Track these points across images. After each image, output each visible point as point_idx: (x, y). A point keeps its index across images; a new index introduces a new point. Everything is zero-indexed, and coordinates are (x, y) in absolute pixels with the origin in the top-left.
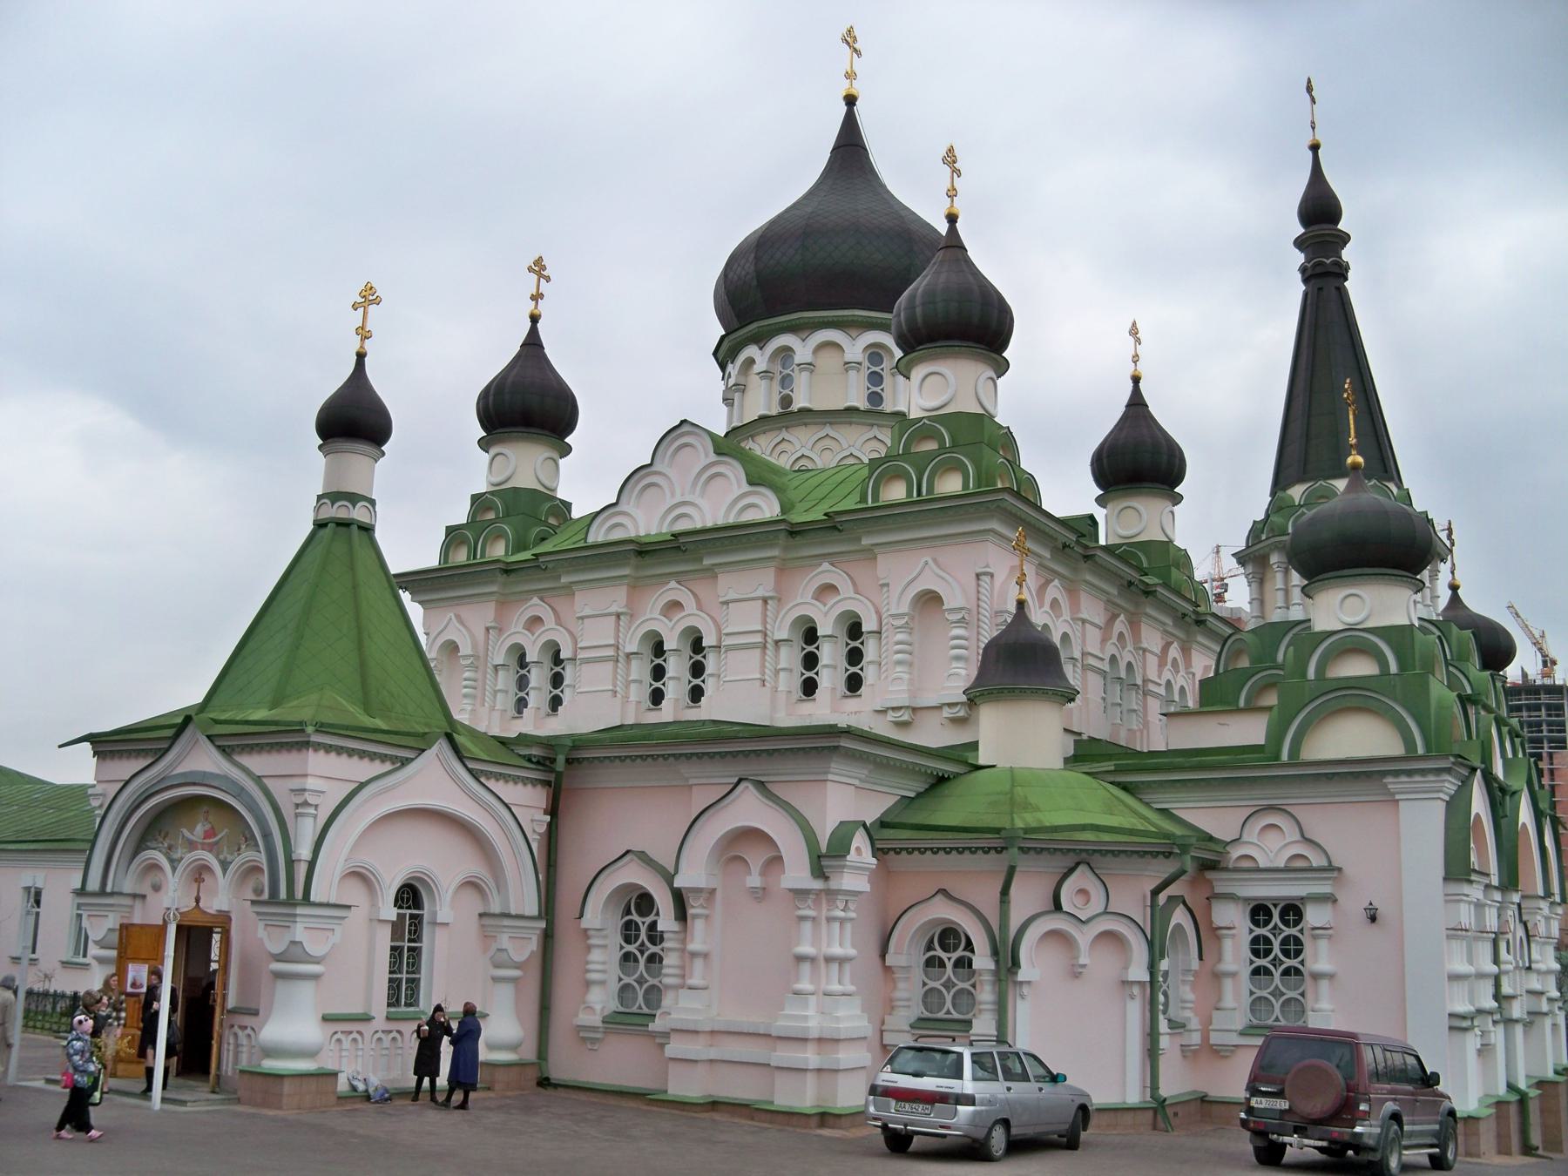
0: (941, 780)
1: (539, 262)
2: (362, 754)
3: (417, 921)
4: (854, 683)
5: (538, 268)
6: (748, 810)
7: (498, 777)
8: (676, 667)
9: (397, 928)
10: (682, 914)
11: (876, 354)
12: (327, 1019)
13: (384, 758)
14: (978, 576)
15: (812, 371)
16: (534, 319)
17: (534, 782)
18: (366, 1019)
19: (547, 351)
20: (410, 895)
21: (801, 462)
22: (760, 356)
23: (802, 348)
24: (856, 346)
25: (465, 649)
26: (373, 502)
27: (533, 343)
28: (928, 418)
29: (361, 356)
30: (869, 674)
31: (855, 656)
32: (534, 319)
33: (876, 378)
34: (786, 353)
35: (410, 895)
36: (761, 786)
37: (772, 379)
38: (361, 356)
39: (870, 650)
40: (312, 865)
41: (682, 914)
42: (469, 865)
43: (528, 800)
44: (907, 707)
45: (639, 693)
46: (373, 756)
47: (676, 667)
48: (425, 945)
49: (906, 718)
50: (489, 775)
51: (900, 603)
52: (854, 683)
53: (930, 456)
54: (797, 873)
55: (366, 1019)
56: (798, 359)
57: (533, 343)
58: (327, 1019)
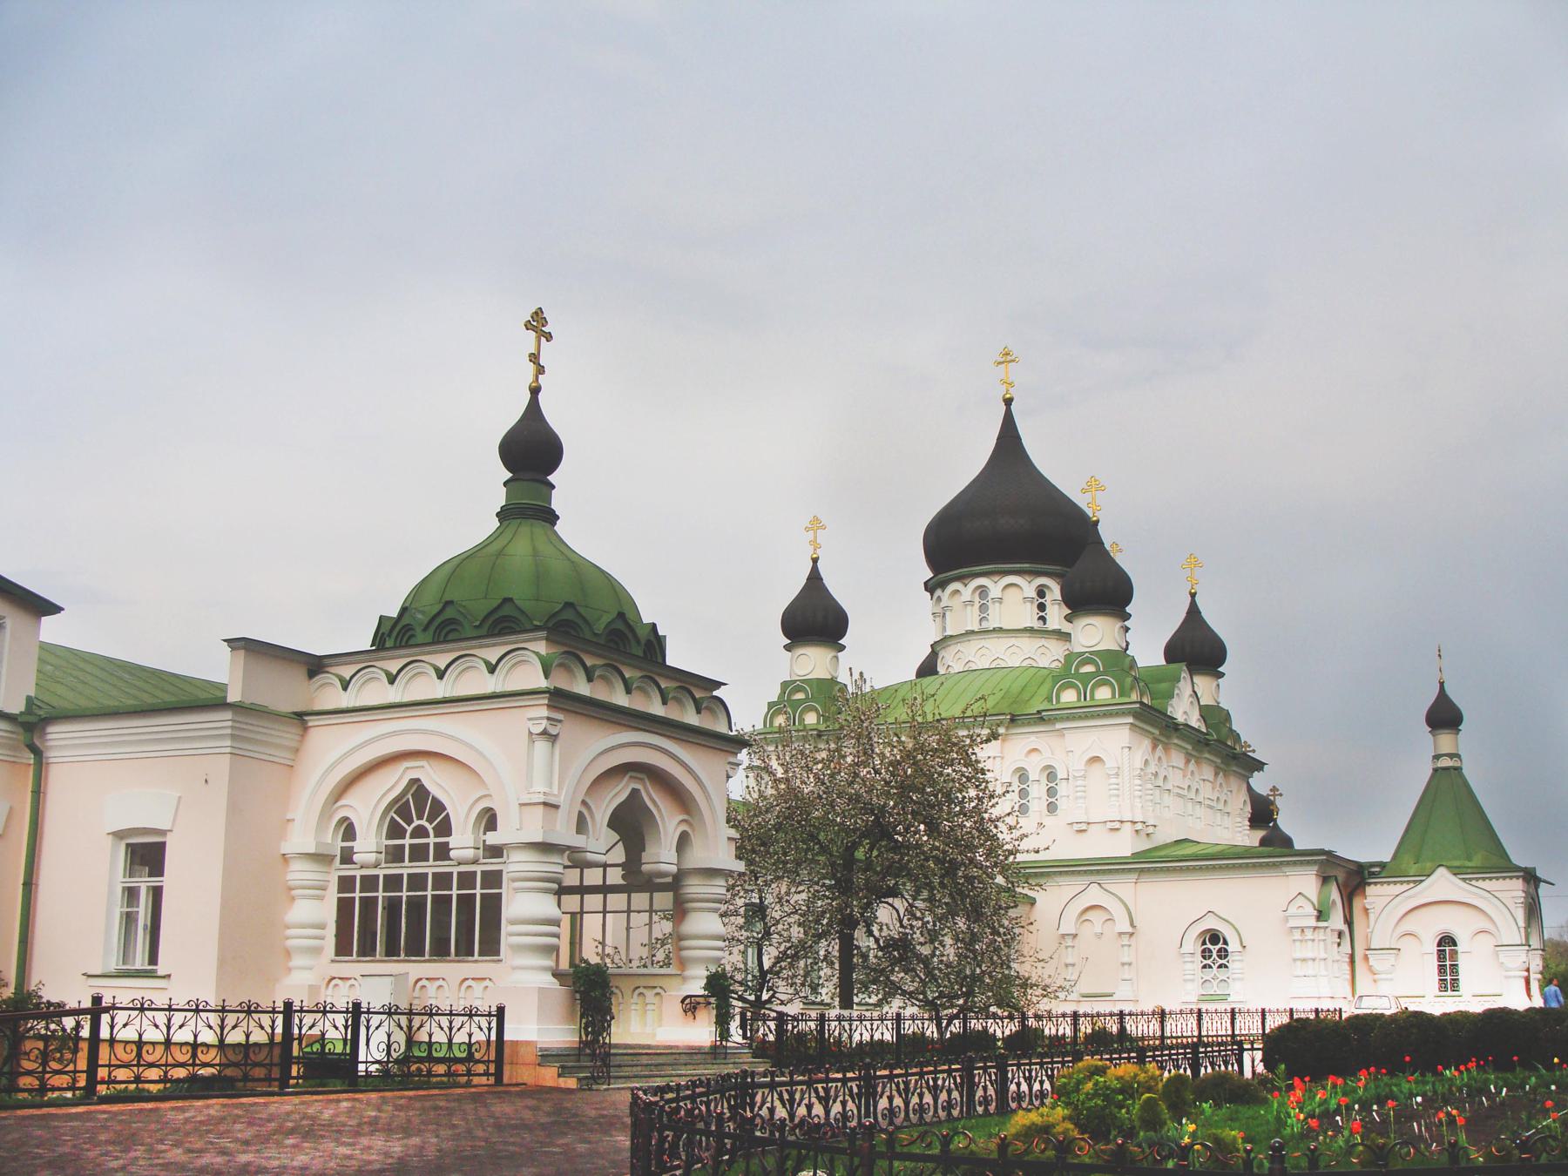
4: (1052, 808)
11: (1041, 593)
14: (1122, 748)
15: (1001, 603)
19: (825, 581)
21: (998, 661)
22: (967, 590)
23: (995, 586)
24: (1028, 587)
28: (1090, 653)
30: (1062, 804)
31: (1051, 792)
33: (1042, 607)
34: (983, 591)
37: (973, 605)
39: (1062, 789)
44: (1085, 822)
49: (1084, 828)
51: (1077, 763)
52: (1052, 808)
53: (1090, 676)
56: (991, 595)
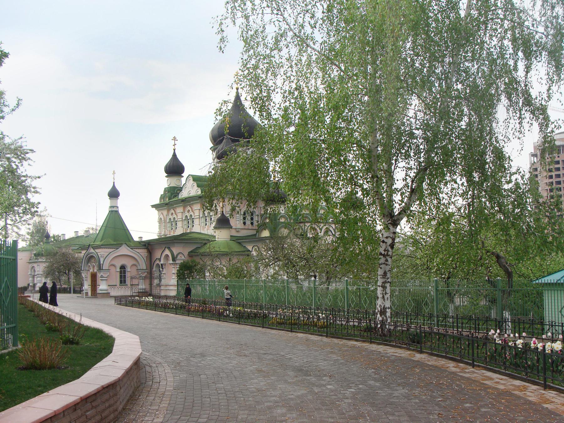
0: (206, 244)
1: (175, 138)
2: (110, 248)
3: (125, 272)
5: (175, 139)
6: (167, 252)
7: (136, 248)
8: (190, 222)
9: (121, 272)
10: (162, 268)
12: (109, 286)
13: (114, 248)
16: (174, 150)
17: (144, 248)
18: (116, 285)
20: (123, 267)
25: (163, 220)
26: (118, 207)
27: (174, 155)
29: (114, 183)
32: (174, 150)
35: (123, 267)
36: (169, 248)
38: (114, 183)
40: (103, 264)
41: (162, 268)
42: (134, 262)
43: (143, 252)
45: (186, 227)
46: (112, 248)
47: (190, 222)
48: (126, 274)
50: (135, 248)
54: (171, 262)
55: (116, 285)
57: (174, 155)
58: (109, 286)
